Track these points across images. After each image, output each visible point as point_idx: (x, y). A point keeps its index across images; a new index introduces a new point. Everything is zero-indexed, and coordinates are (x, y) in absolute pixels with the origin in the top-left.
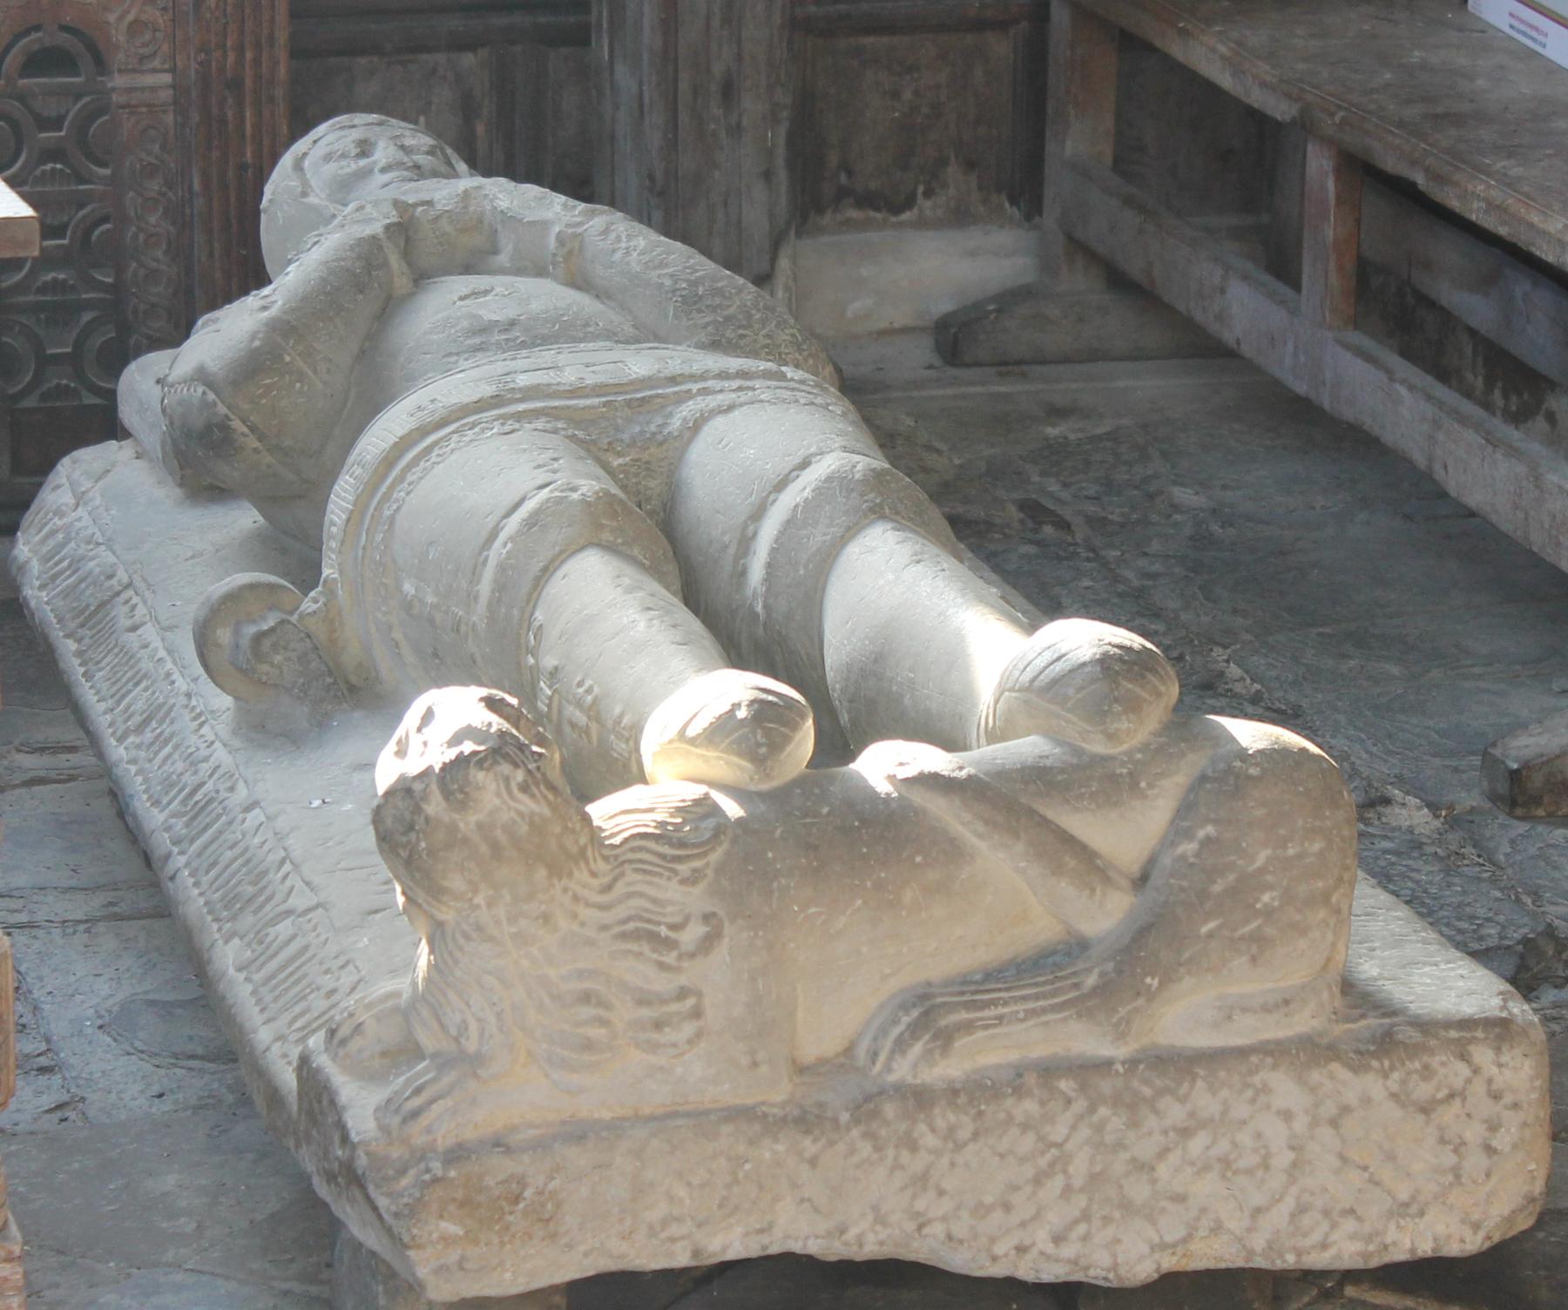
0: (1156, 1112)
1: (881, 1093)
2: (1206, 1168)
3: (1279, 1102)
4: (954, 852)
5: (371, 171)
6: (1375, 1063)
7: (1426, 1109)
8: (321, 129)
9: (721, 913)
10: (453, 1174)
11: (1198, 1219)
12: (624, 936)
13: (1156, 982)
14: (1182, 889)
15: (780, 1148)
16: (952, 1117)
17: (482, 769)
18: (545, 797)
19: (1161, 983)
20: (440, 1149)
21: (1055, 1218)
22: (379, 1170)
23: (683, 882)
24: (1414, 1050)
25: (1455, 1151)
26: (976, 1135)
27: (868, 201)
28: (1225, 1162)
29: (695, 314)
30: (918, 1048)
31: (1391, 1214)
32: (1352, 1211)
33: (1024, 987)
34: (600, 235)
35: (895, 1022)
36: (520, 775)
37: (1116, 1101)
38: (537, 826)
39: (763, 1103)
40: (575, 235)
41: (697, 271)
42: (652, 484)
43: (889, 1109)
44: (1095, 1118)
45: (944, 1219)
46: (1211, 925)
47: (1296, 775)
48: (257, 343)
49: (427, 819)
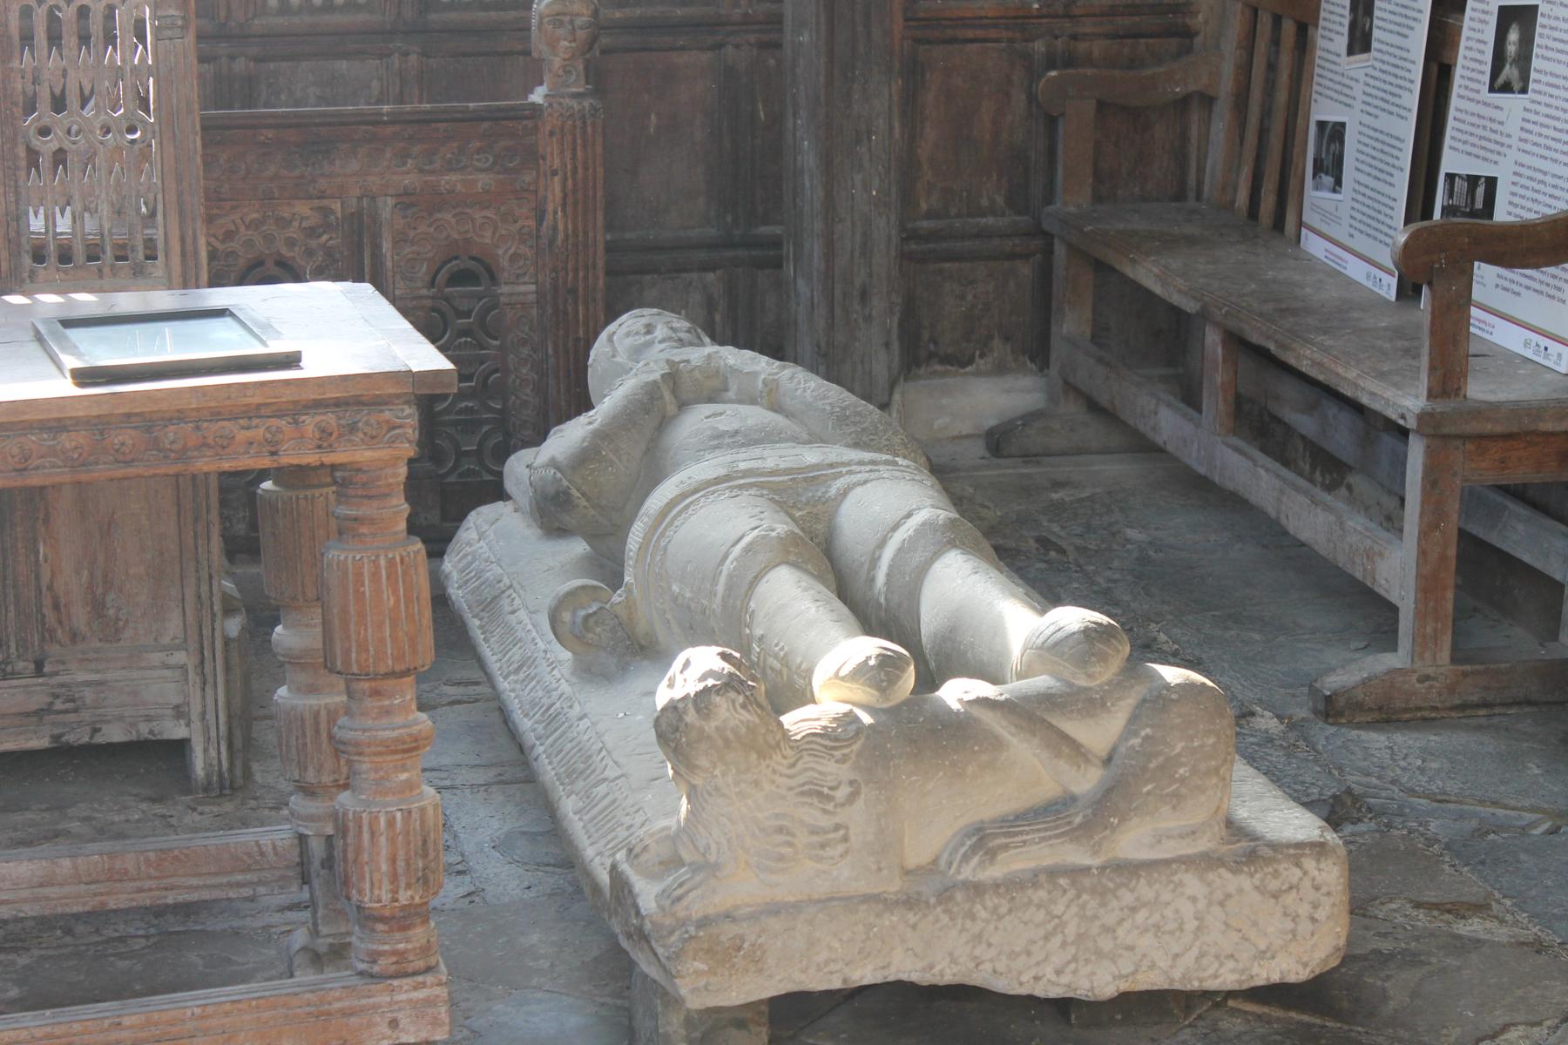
0: (1117, 898)
1: (954, 886)
2: (1146, 930)
3: (1189, 891)
4: (997, 744)
5: (653, 342)
6: (1246, 869)
7: (1276, 896)
8: (624, 317)
9: (860, 780)
10: (701, 934)
11: (1141, 960)
12: (802, 794)
13: (1116, 821)
14: (1132, 766)
15: (894, 918)
16: (996, 901)
17: (718, 695)
18: (756, 712)
19: (1119, 822)
20: (694, 919)
21: (1057, 960)
22: (658, 932)
23: (837, 761)
24: (1268, 861)
25: (1293, 920)
26: (1010, 911)
27: (947, 360)
28: (1157, 927)
29: (844, 427)
30: (976, 860)
31: (1255, 958)
32: (1232, 956)
33: (1038, 823)
35: (962, 844)
36: (741, 699)
37: (1093, 891)
38: (752, 729)
39: (884, 892)
40: (774, 380)
42: (819, 527)
43: (959, 896)
44: (1081, 901)
45: (992, 960)
46: (1149, 787)
47: (1199, 698)
48: (586, 444)
49: (686, 725)
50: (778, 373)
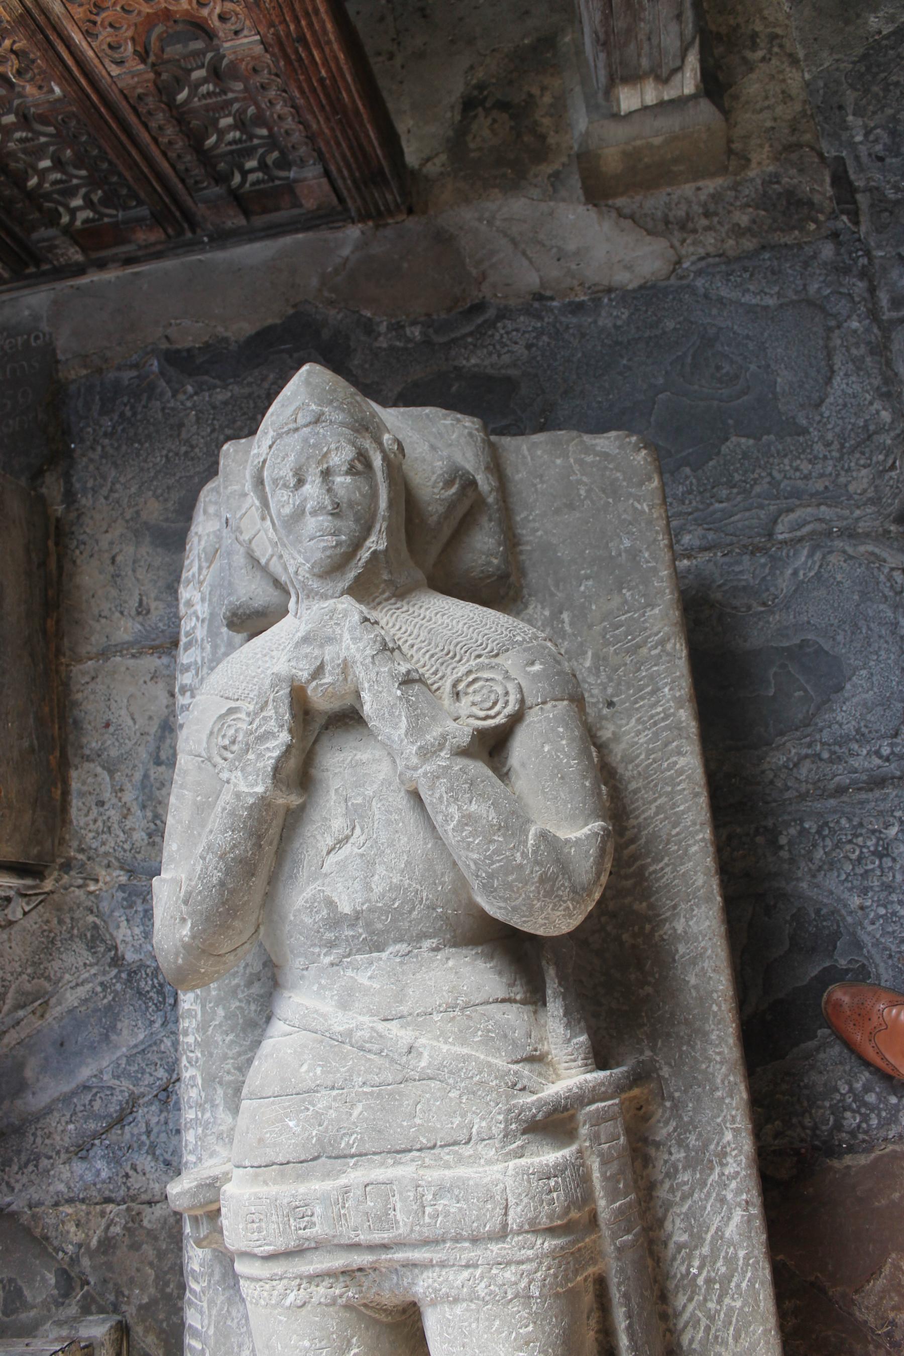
41: (493, 863)
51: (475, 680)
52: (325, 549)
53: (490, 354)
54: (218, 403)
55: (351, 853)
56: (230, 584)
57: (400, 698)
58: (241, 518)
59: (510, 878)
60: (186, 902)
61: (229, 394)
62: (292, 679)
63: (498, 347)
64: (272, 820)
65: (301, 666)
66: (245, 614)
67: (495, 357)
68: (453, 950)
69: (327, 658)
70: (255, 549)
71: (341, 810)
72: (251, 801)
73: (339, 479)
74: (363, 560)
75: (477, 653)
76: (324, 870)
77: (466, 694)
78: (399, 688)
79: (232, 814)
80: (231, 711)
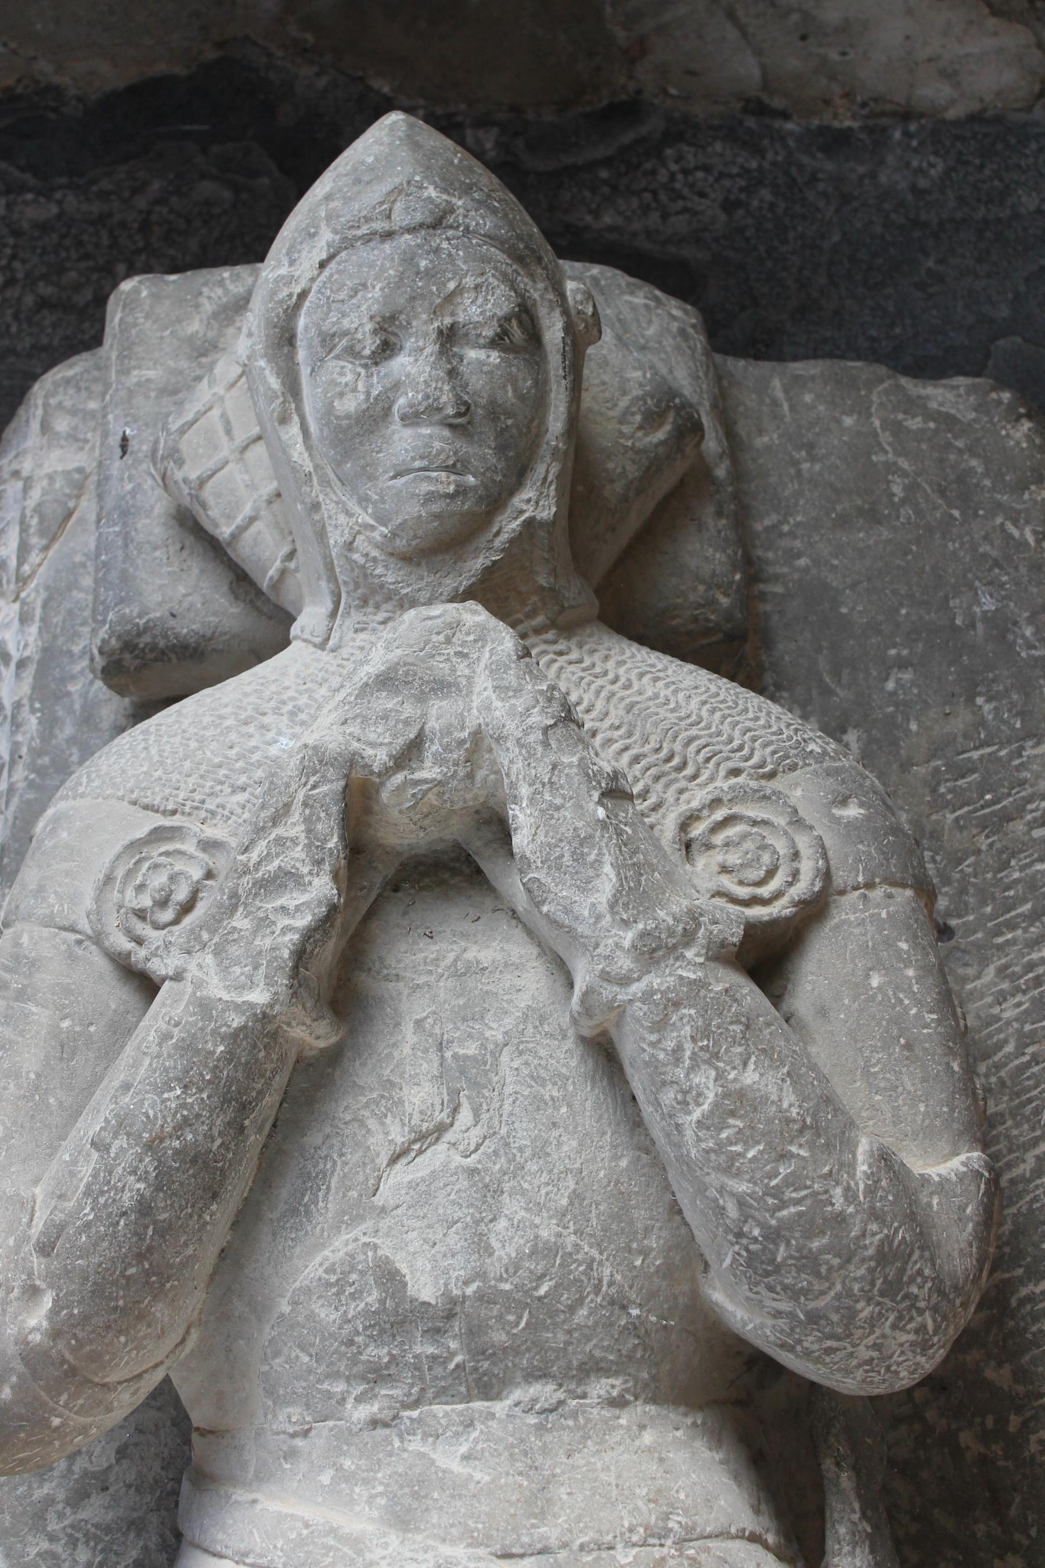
29: (761, 1288)
34: (651, 1030)
40: (610, 1006)
41: (783, 1205)
50: (625, 981)
51: (729, 821)
52: (430, 498)
53: (646, 209)
54: (26, 226)
55: (445, 1166)
56: (125, 578)
57: (604, 825)
58: (183, 431)
59: (815, 1244)
60: (45, 1249)
61: (55, 210)
62: (352, 761)
63: (663, 197)
64: (274, 1072)
65: (372, 737)
66: (154, 647)
67: (655, 217)
68: (652, 1409)
69: (433, 724)
70: (211, 501)
71: (429, 1066)
72: (236, 1021)
73: (473, 354)
74: (504, 536)
75: (731, 764)
76: (379, 1200)
77: (709, 847)
78: (600, 803)
79: (188, 1047)
80: (159, 835)
